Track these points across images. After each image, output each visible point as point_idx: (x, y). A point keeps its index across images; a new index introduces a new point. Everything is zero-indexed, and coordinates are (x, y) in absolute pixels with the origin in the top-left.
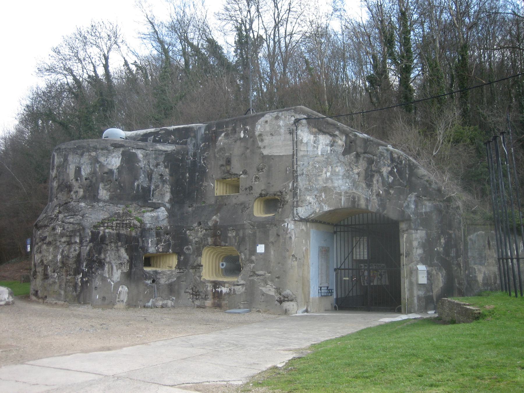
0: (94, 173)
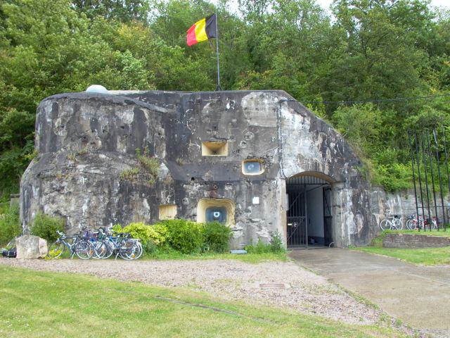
0: (112, 126)
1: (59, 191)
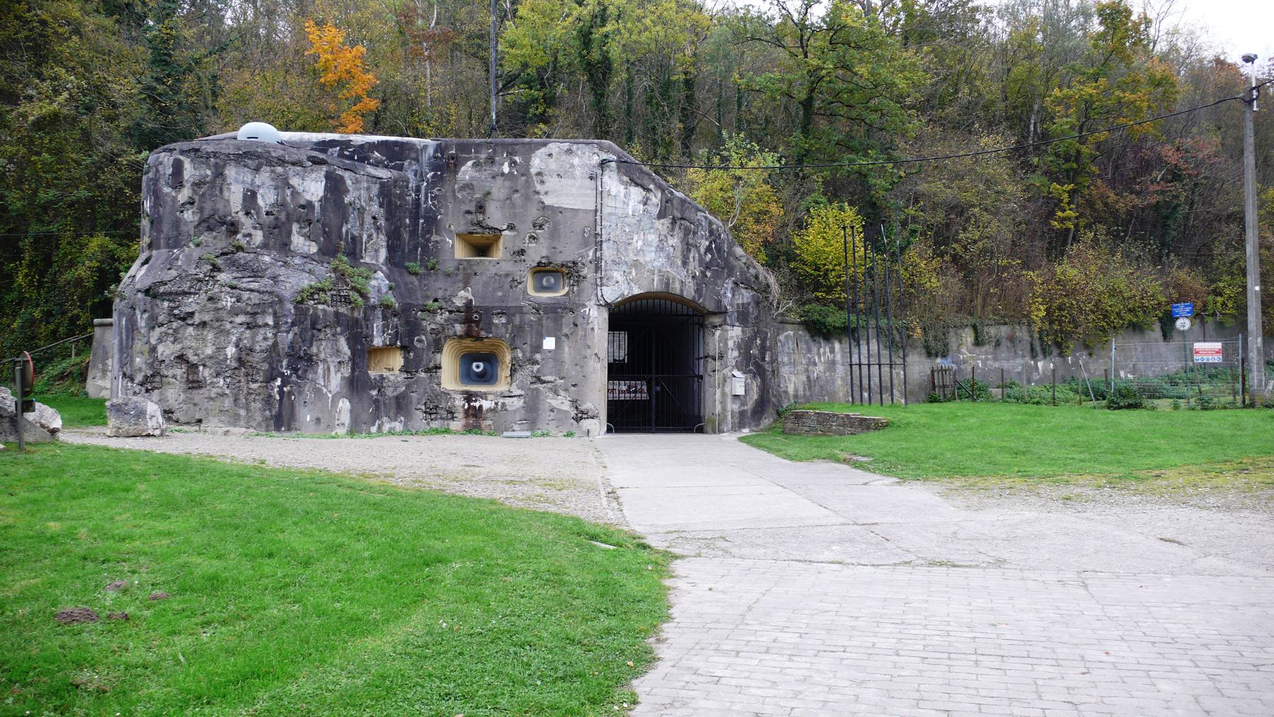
0: (282, 205)
1: (183, 319)
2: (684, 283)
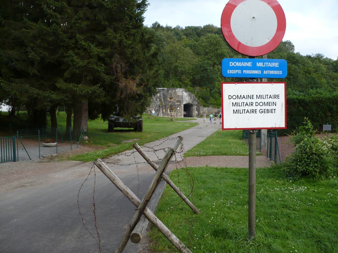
2: (191, 102)
